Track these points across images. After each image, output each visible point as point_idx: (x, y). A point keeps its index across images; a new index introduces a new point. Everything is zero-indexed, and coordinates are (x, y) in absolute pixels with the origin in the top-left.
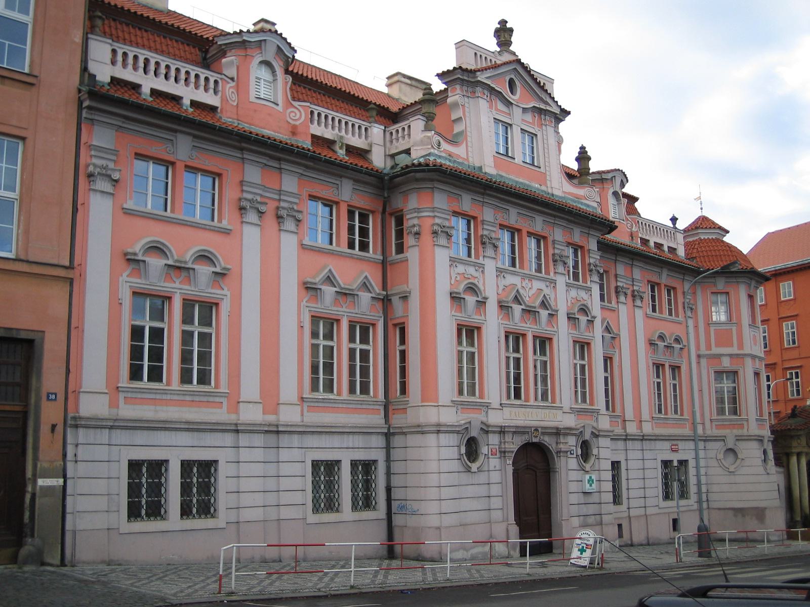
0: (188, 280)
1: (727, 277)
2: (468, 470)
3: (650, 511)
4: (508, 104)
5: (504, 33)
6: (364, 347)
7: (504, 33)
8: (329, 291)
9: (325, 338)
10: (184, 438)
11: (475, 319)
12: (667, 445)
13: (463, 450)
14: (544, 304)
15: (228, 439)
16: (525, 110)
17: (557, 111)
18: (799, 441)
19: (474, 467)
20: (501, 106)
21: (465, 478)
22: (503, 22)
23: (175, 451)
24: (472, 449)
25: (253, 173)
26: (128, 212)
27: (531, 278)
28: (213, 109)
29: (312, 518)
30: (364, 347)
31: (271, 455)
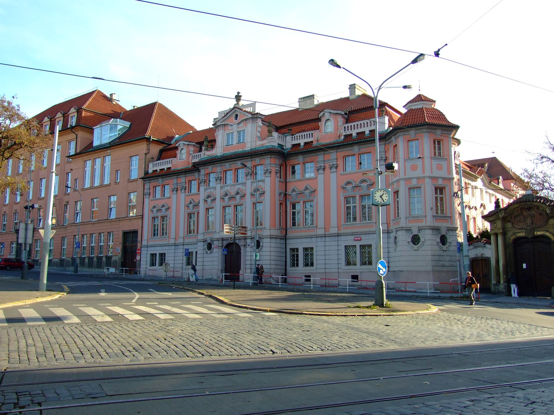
0: (161, 212)
1: (394, 135)
2: (207, 253)
3: (340, 270)
4: (232, 125)
5: (238, 97)
6: (441, 196)
7: (238, 97)
8: (191, 206)
9: (440, 194)
10: (160, 248)
11: (212, 206)
12: (352, 237)
13: (206, 247)
14: (238, 193)
15: (168, 248)
16: (238, 124)
17: (250, 116)
18: (495, 225)
19: (209, 252)
20: (230, 127)
21: (206, 255)
22: (238, 93)
23: (158, 251)
24: (210, 246)
25: (175, 181)
26: (152, 200)
27: (234, 185)
28: (170, 168)
29: (184, 267)
30: (441, 196)
31: (176, 251)
